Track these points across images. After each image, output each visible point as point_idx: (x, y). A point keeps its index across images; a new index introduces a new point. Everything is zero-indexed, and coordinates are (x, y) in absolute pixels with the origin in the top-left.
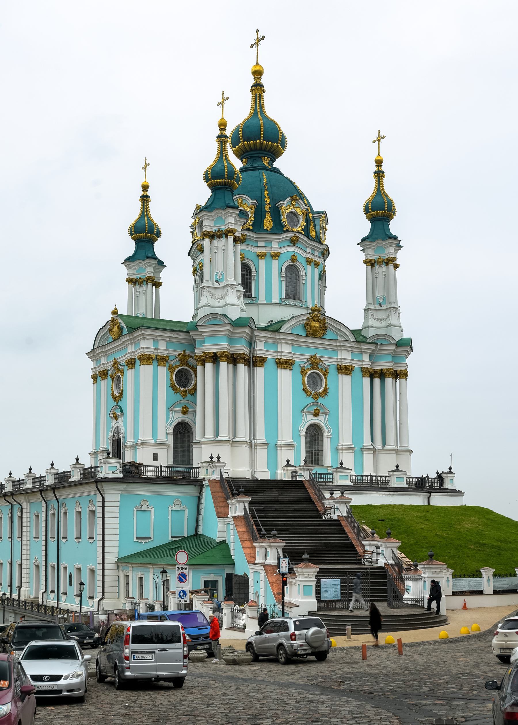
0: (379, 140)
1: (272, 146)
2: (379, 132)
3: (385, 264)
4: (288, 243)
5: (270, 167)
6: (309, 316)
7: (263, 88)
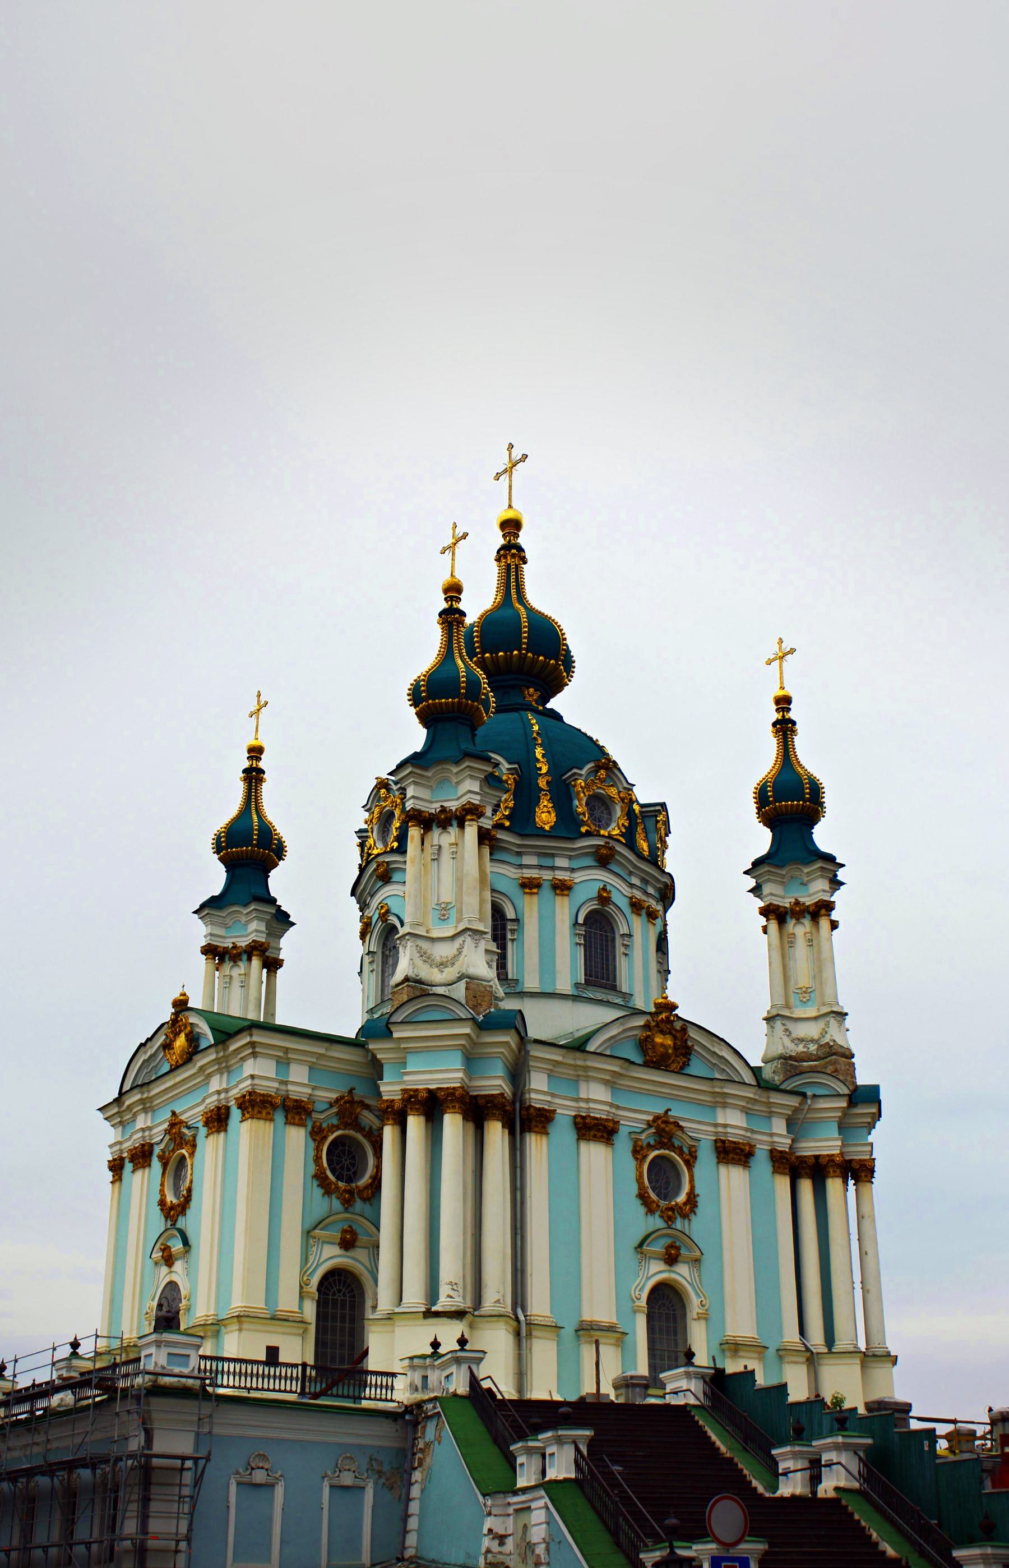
0: (782, 658)
1: (545, 665)
2: (781, 641)
3: (808, 917)
4: (589, 861)
5: (541, 708)
6: (649, 1017)
7: (523, 554)
